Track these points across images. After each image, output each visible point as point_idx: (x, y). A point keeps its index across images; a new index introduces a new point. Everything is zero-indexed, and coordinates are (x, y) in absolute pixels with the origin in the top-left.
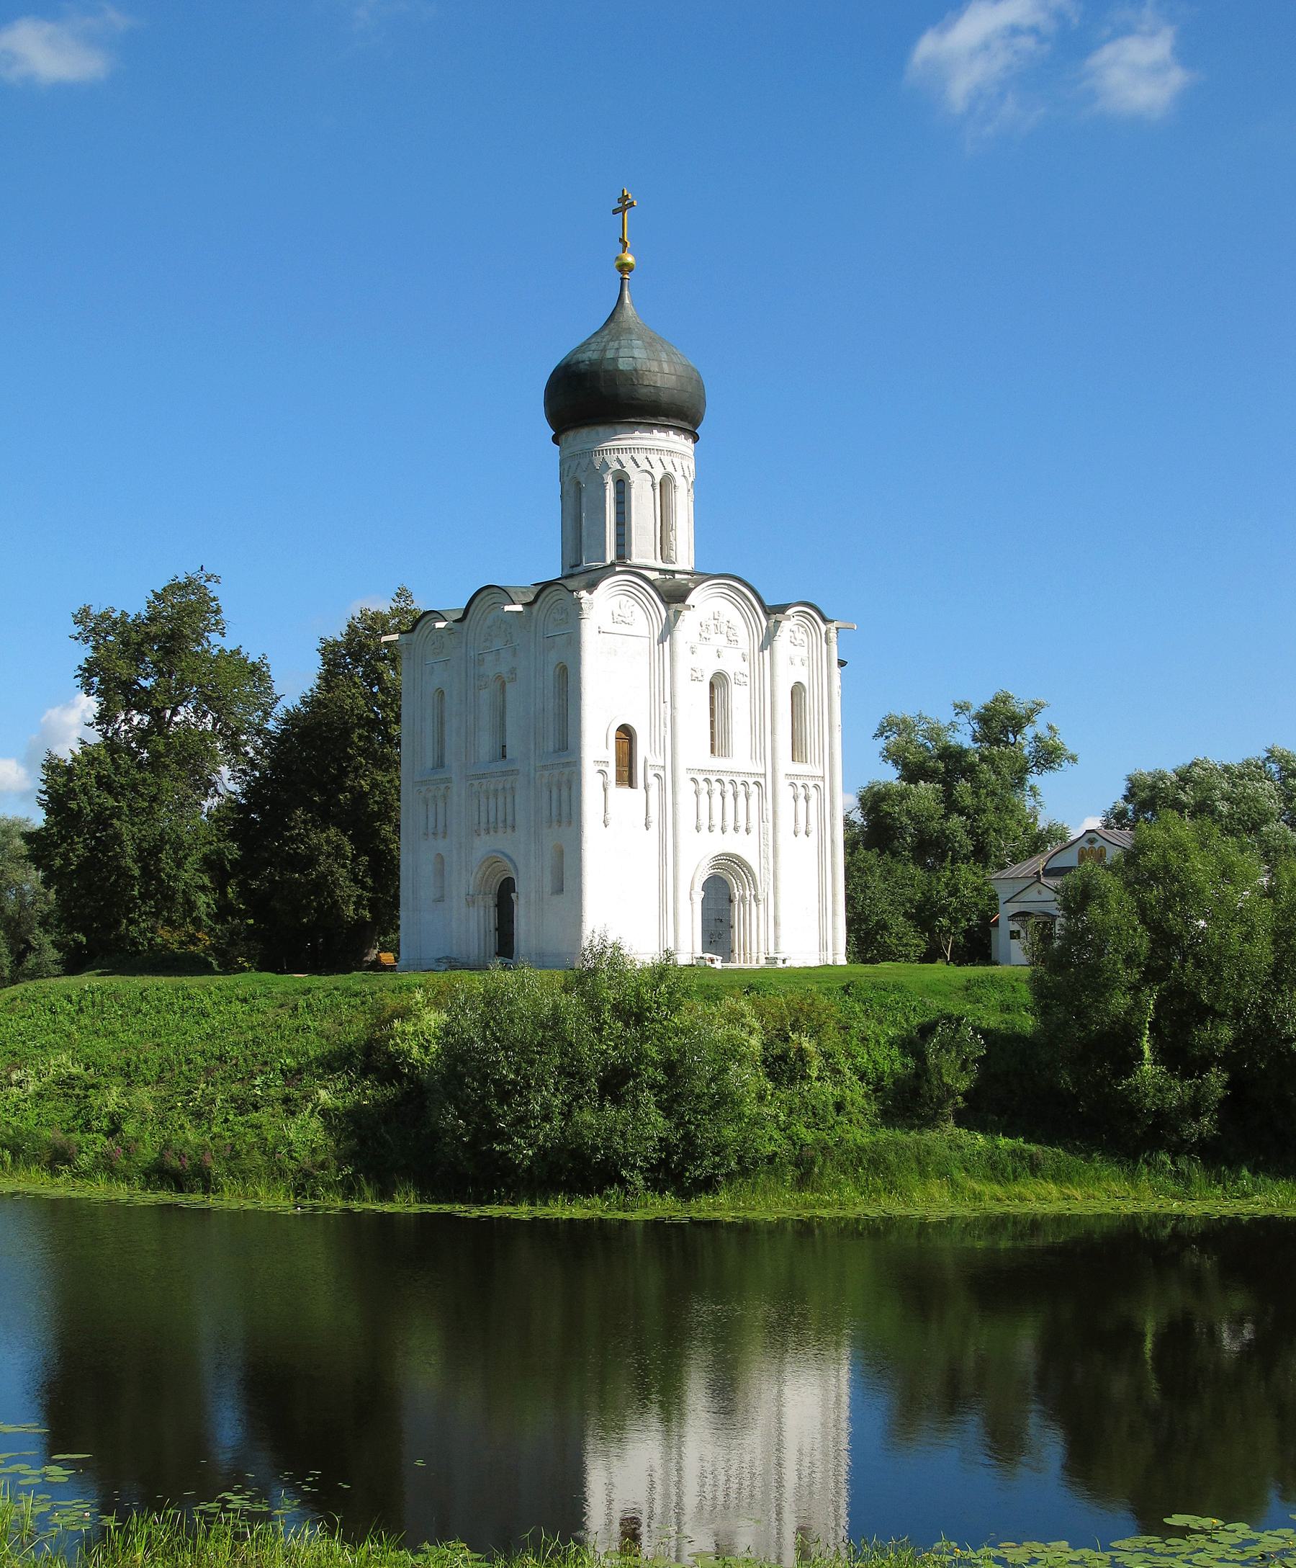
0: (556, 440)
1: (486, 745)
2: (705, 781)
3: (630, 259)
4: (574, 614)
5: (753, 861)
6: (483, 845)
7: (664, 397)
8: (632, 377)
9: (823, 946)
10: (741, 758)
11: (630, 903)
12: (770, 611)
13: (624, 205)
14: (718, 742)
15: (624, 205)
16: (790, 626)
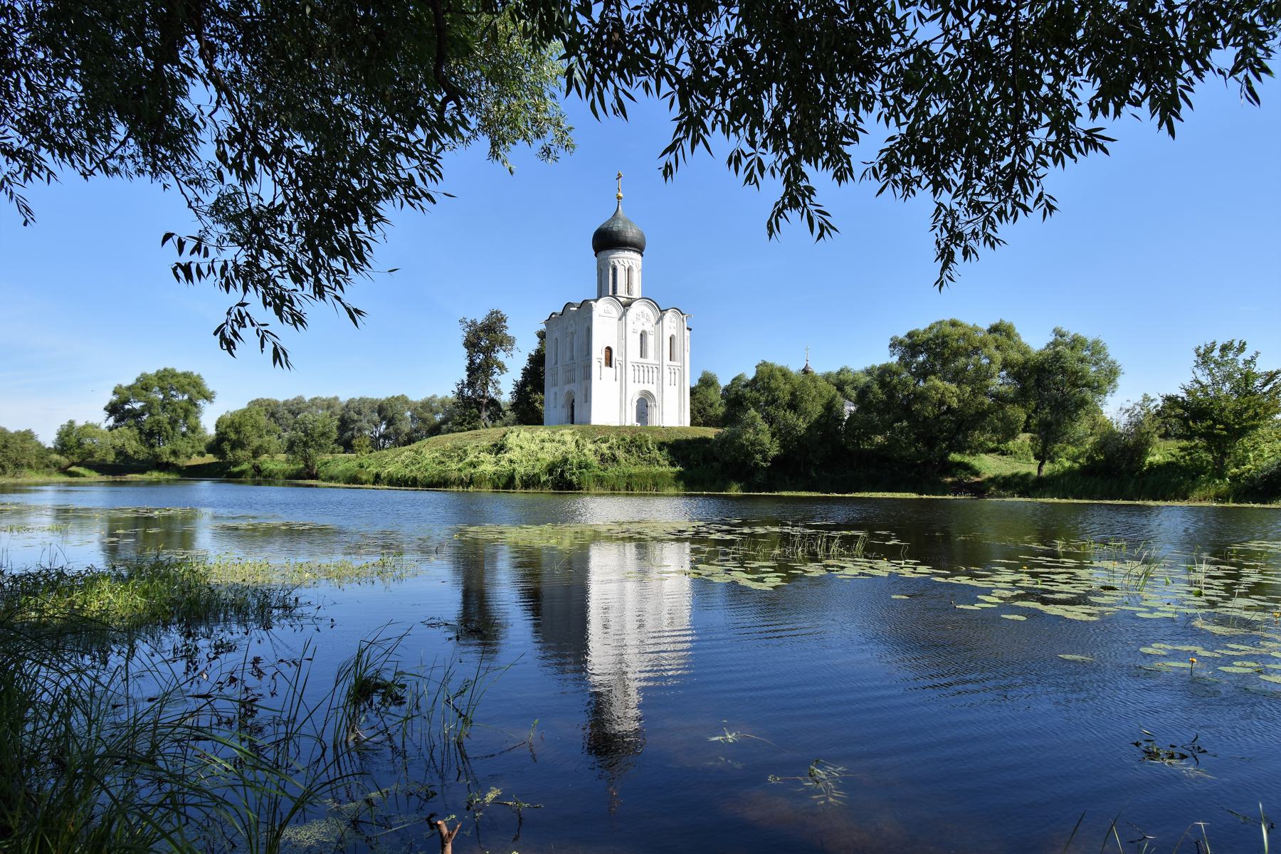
2: (637, 366)
4: (590, 309)
5: (654, 392)
6: (568, 388)
11: (609, 404)
13: (619, 176)
14: (643, 353)
15: (619, 176)
16: (669, 315)
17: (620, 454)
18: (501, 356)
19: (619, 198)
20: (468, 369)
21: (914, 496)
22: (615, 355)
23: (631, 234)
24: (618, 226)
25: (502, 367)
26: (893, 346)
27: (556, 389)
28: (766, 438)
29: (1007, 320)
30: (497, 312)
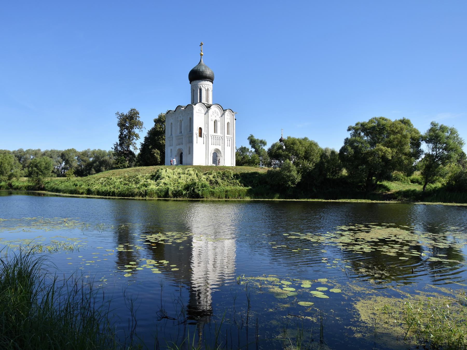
0: (190, 83)
1: (178, 131)
2: (213, 137)
3: (202, 53)
4: (192, 109)
5: (221, 150)
6: (178, 147)
7: (208, 76)
8: (202, 72)
9: (232, 164)
10: (219, 133)
11: (201, 156)
12: (224, 111)
13: (201, 44)
14: (215, 131)
15: (201, 44)
16: (227, 113)
17: (219, 180)
18: (136, 131)
19: (201, 55)
20: (120, 137)
21: (370, 201)
22: (203, 132)
23: (208, 73)
24: (202, 69)
25: (137, 136)
26: (349, 130)
27: (171, 148)
28: (294, 173)
29: (407, 118)
30: (134, 110)
